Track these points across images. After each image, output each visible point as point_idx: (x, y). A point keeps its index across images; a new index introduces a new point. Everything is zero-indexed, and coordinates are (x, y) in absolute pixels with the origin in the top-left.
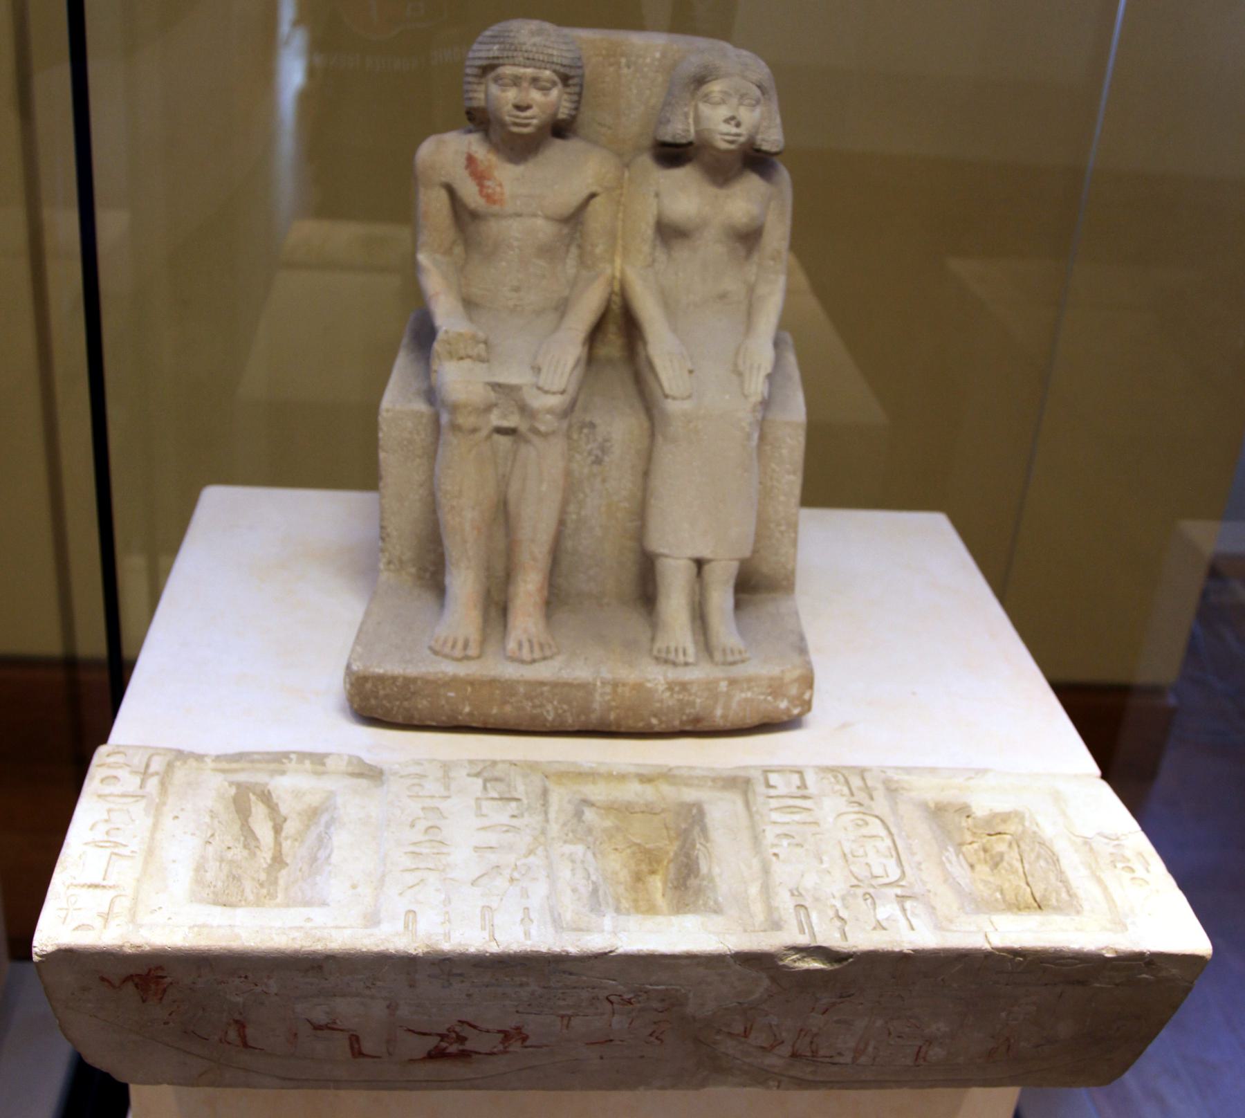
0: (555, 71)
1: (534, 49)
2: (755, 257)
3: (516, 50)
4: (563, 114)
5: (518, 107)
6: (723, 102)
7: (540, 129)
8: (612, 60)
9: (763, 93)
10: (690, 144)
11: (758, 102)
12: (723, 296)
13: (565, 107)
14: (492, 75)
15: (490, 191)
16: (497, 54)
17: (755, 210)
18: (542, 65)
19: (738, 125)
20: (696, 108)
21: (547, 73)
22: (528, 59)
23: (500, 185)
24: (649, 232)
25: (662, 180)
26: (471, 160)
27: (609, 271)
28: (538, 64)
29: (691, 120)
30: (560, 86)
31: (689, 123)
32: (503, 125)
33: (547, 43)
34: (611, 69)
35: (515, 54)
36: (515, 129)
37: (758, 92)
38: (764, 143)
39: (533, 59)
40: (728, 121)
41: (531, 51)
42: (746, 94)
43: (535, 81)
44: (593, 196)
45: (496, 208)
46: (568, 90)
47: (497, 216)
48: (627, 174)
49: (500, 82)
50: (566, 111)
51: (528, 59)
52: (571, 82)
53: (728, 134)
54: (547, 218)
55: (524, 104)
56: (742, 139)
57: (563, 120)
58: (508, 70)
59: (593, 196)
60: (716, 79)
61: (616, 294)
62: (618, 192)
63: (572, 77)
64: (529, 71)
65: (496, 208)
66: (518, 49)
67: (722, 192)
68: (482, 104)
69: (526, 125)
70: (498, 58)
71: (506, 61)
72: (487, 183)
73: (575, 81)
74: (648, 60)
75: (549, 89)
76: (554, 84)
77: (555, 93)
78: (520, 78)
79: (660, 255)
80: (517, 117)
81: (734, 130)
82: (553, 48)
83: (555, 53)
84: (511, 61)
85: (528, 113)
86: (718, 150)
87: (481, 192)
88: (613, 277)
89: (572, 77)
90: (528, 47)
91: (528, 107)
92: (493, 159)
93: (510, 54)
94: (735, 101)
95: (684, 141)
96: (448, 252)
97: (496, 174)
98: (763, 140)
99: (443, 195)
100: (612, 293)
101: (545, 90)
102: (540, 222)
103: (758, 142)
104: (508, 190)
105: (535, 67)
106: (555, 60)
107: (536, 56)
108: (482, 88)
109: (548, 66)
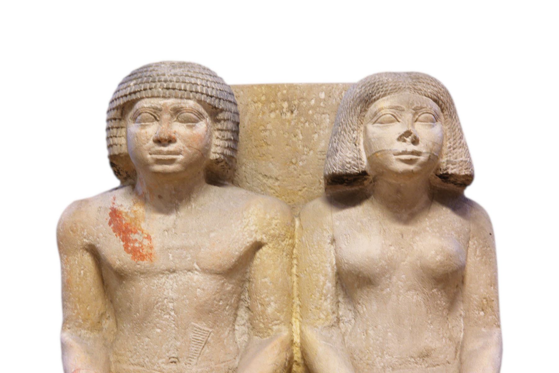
0: (199, 101)
1: (175, 79)
2: (461, 309)
3: (154, 82)
4: (215, 153)
5: (159, 141)
6: (395, 119)
7: (189, 165)
8: (273, 105)
9: (442, 110)
10: (364, 173)
11: (436, 119)
12: (425, 355)
13: (217, 146)
14: (131, 114)
15: (137, 245)
16: (133, 89)
17: (451, 246)
18: (186, 94)
19: (415, 142)
20: (366, 131)
21: (191, 103)
22: (168, 89)
23: (149, 238)
24: (329, 285)
25: (337, 223)
26: (115, 214)
27: (285, 333)
28: (180, 93)
29: (362, 147)
30: (208, 120)
31: (359, 150)
32: (146, 165)
33: (189, 74)
34: (273, 115)
35: (153, 85)
36: (158, 168)
37: (436, 107)
38: (450, 166)
39: (174, 89)
40: (402, 138)
41: (171, 81)
42: (421, 108)
43: (177, 111)
44: (258, 246)
45: (145, 264)
46: (219, 126)
47: (144, 273)
48: (297, 223)
49: (139, 118)
50: (219, 150)
51: (168, 89)
52: (221, 116)
53: (404, 153)
54: (204, 271)
55: (165, 136)
56: (422, 159)
57: (217, 161)
58: (145, 104)
59: (258, 246)
60: (384, 95)
61: (298, 364)
62: (288, 241)
63: (222, 110)
64: (171, 102)
65: (145, 264)
66: (157, 80)
67: (411, 228)
68: (124, 150)
69: (172, 161)
70: (135, 93)
71: (143, 94)
72: (133, 236)
73: (225, 115)
74: (313, 102)
75: (196, 121)
76: (200, 116)
77: (202, 127)
78: (160, 110)
79: (344, 311)
80: (160, 153)
81: (411, 147)
82: (197, 78)
83: (199, 82)
84: (149, 93)
85: (172, 147)
86: (398, 174)
87: (126, 247)
88: (292, 342)
89: (222, 110)
90: (167, 77)
91: (171, 141)
92: (140, 210)
93: (148, 86)
94: (408, 116)
95: (356, 170)
96: (96, 327)
97: (143, 225)
98: (448, 162)
99: (88, 258)
100: (291, 361)
101: (190, 122)
102: (197, 277)
103: (444, 166)
104: (157, 243)
105: (176, 97)
106: (199, 89)
107: (177, 85)
108: (123, 131)
109: (191, 95)
